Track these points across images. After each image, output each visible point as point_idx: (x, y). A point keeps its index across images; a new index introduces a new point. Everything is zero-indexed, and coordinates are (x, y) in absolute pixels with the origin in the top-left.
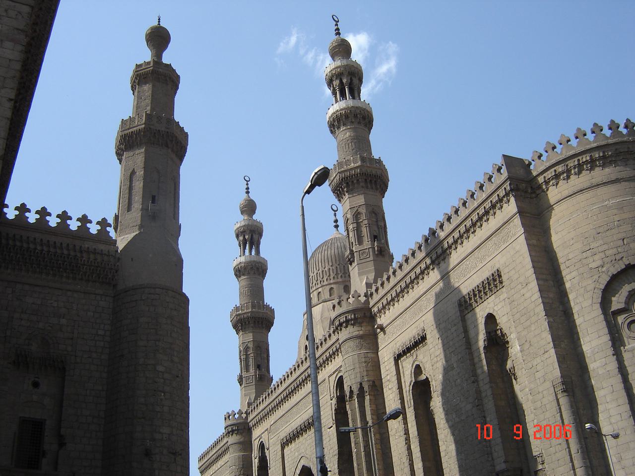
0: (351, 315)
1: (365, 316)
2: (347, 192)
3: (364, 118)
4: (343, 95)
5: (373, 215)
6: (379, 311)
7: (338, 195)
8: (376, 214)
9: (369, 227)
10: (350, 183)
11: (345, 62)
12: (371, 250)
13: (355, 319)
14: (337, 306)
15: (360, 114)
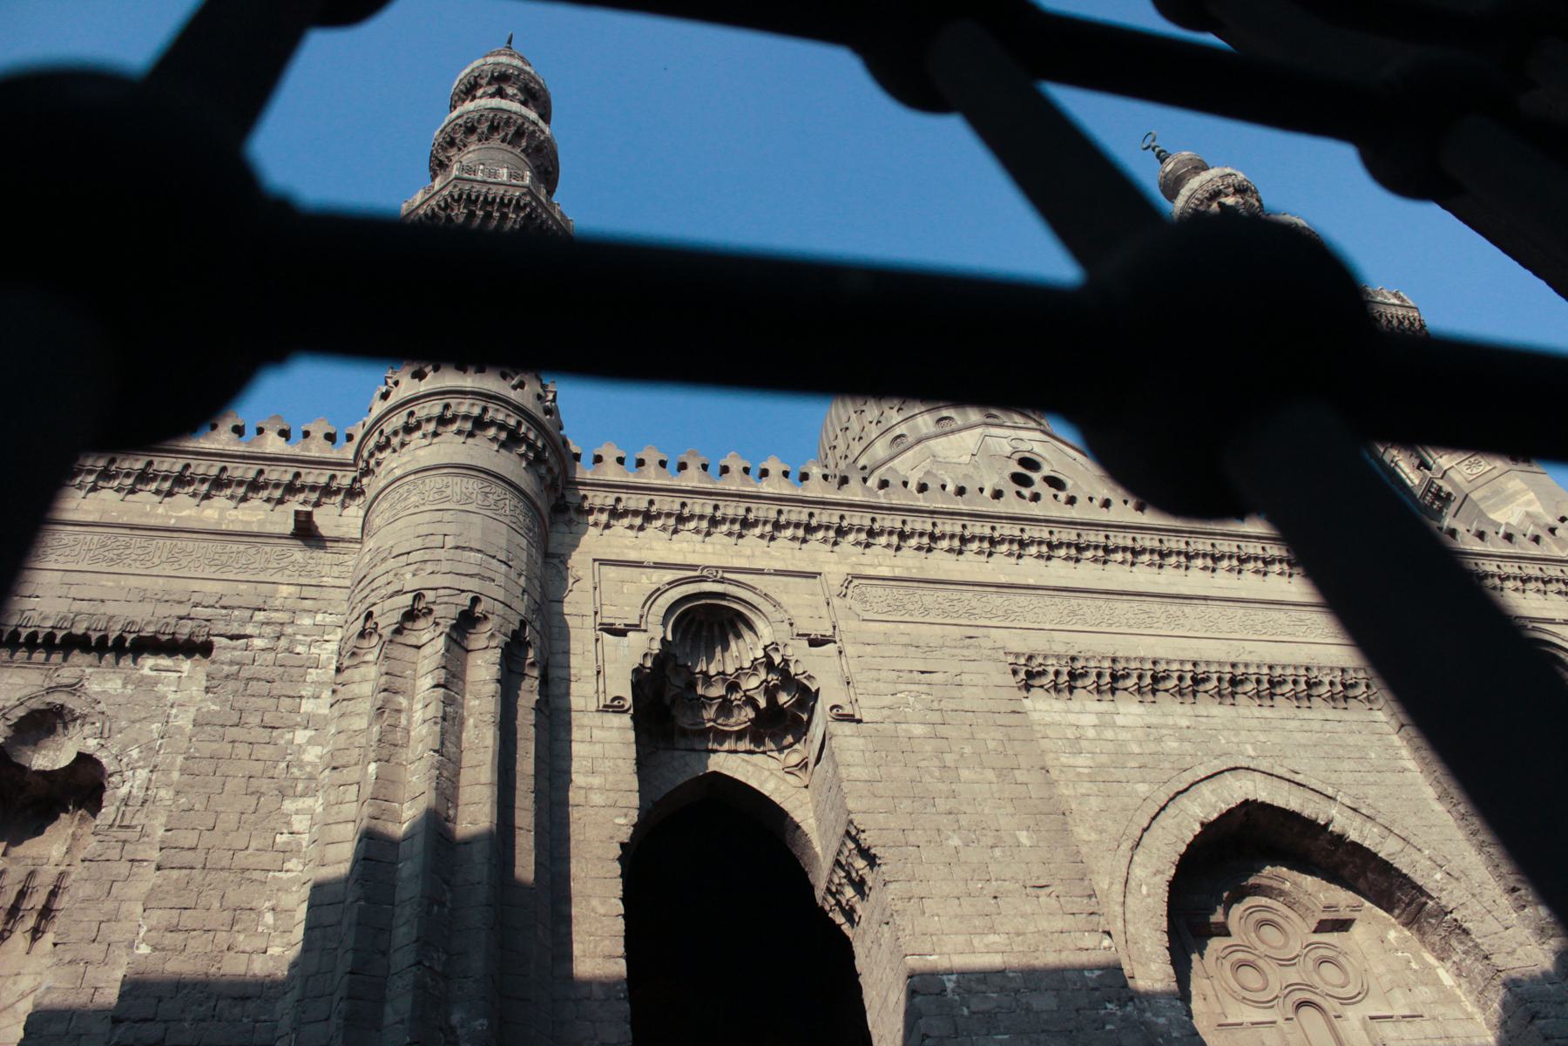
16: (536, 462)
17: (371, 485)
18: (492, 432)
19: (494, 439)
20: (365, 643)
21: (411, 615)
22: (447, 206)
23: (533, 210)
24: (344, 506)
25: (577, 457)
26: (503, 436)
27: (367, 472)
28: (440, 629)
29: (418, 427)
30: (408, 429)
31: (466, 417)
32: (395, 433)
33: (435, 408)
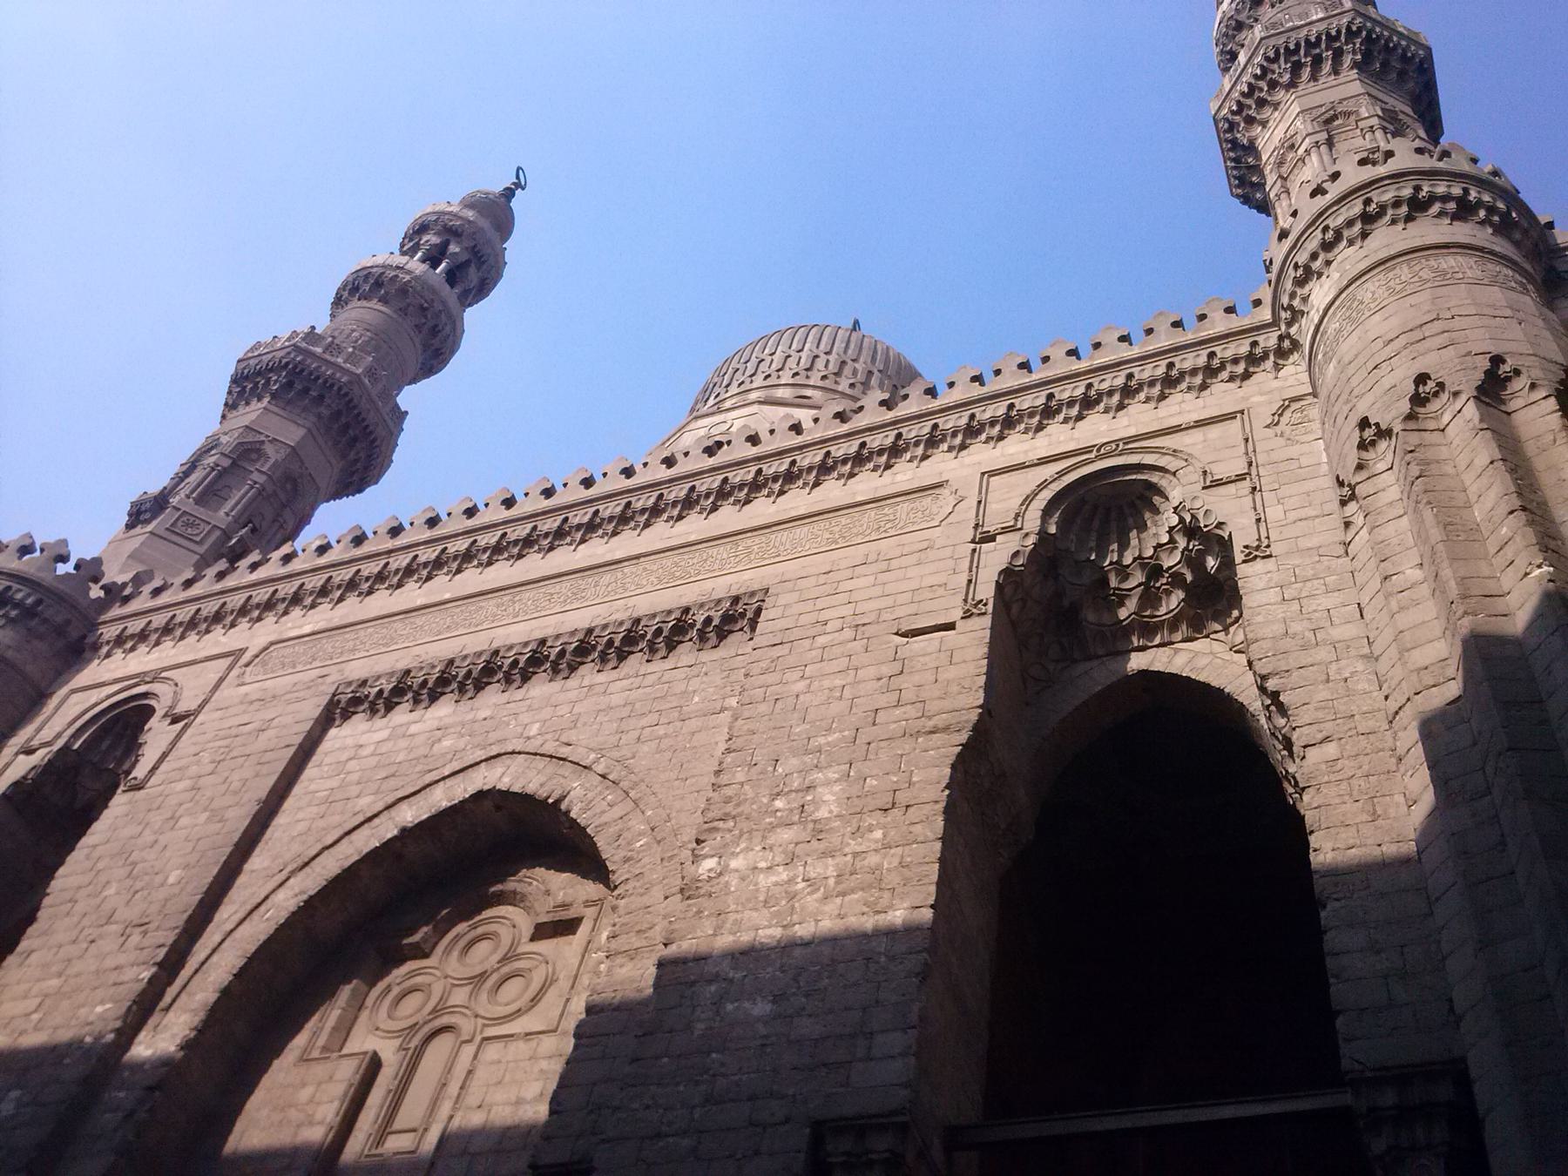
0: (29, 595)
1: (60, 631)
2: (274, 396)
3: (434, 331)
4: (433, 259)
5: (289, 486)
6: (119, 641)
7: (242, 393)
8: (295, 489)
9: (260, 493)
10: (298, 386)
11: (484, 223)
12: (218, 533)
13: (29, 613)
14: (12, 551)
15: (437, 315)
16: (1504, 227)
17: (1304, 330)
18: (1436, 208)
19: (1441, 214)
20: (1369, 455)
21: (1418, 400)
22: (1264, 70)
23: (1370, 32)
24: (1278, 367)
25: (1550, 225)
26: (1452, 206)
27: (1296, 315)
28: (1464, 397)
29: (1338, 236)
30: (1327, 246)
31: (1397, 204)
32: (1314, 256)
33: (1356, 208)
